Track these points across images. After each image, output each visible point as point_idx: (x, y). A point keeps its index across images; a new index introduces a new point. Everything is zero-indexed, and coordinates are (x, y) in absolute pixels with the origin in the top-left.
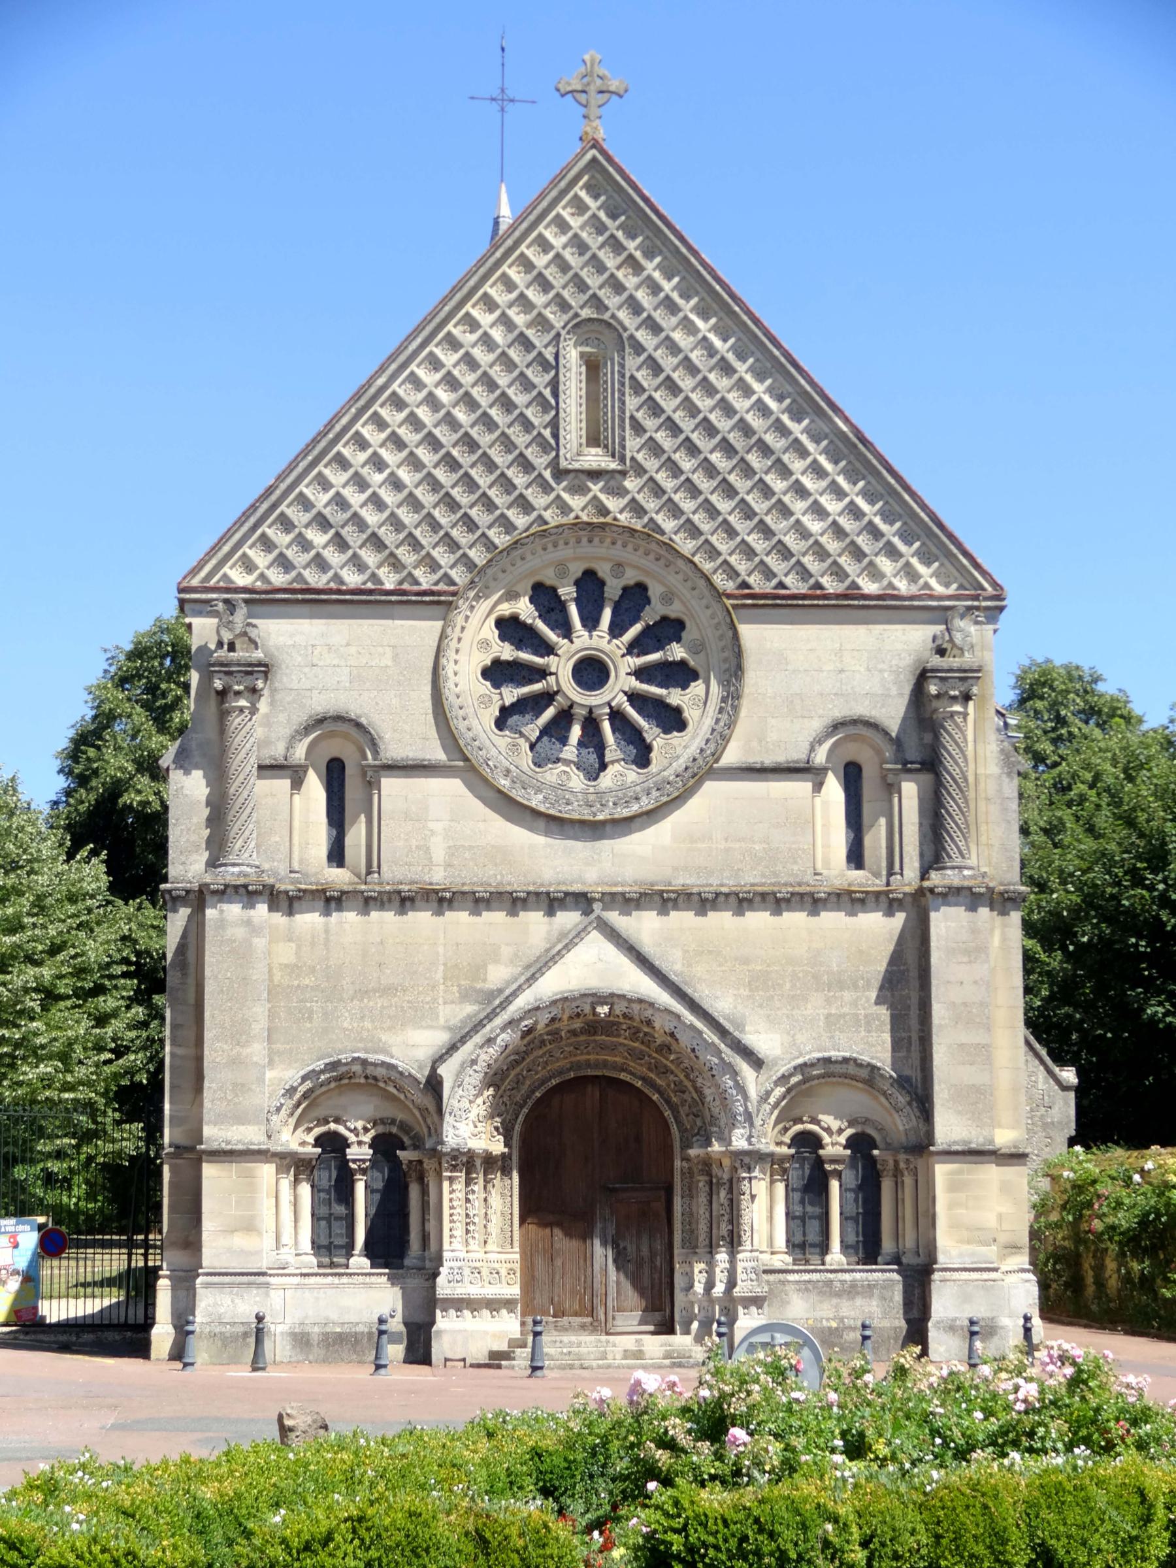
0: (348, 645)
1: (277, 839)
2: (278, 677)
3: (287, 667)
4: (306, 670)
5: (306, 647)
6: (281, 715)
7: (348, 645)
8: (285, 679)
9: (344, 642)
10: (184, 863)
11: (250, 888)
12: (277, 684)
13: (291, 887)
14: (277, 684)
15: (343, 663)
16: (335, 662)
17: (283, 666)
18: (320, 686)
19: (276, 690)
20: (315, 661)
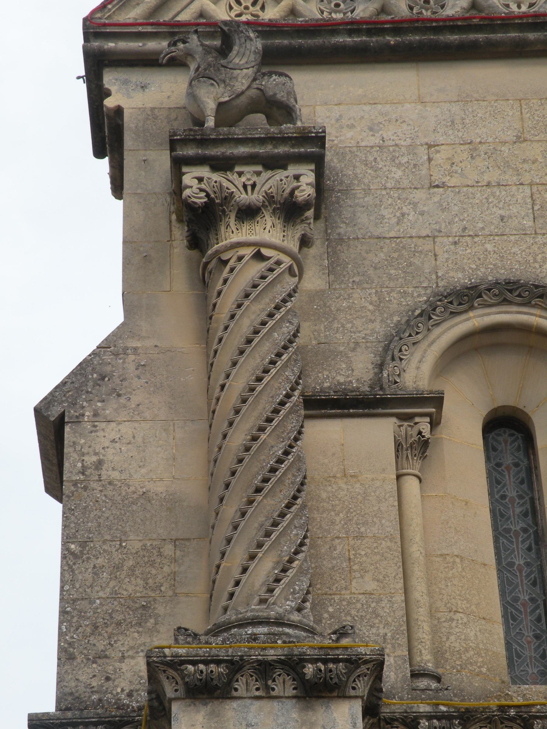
0: (520, 139)
1: (371, 586)
2: (347, 214)
3: (367, 191)
4: (419, 195)
5: (412, 148)
6: (357, 294)
7: (520, 139)
8: (363, 219)
9: (510, 136)
10: (102, 656)
11: (309, 670)
12: (343, 229)
13: (424, 708)
14: (343, 229)
15: (509, 177)
16: (493, 176)
17: (358, 191)
18: (456, 229)
19: (341, 240)
20: (437, 178)
